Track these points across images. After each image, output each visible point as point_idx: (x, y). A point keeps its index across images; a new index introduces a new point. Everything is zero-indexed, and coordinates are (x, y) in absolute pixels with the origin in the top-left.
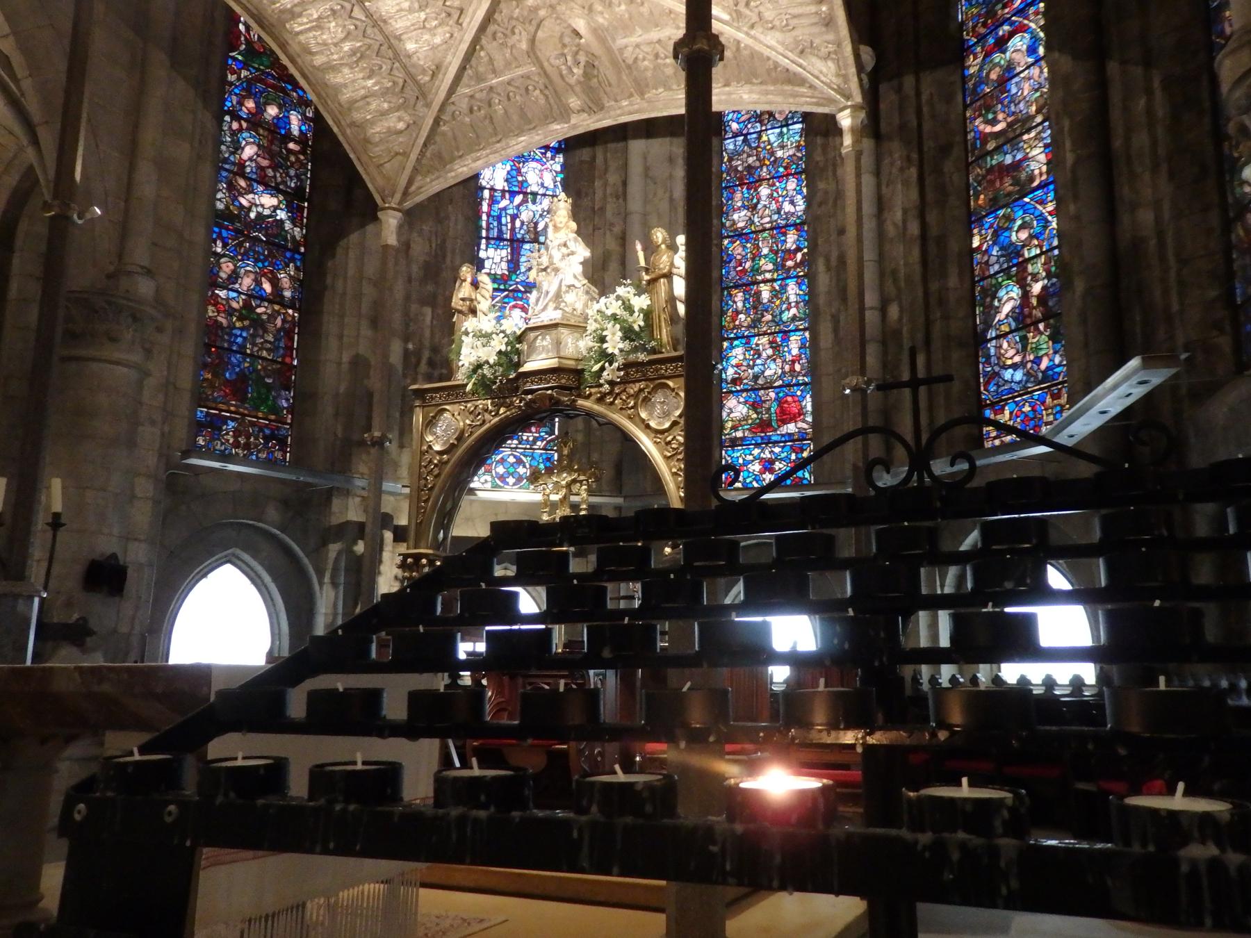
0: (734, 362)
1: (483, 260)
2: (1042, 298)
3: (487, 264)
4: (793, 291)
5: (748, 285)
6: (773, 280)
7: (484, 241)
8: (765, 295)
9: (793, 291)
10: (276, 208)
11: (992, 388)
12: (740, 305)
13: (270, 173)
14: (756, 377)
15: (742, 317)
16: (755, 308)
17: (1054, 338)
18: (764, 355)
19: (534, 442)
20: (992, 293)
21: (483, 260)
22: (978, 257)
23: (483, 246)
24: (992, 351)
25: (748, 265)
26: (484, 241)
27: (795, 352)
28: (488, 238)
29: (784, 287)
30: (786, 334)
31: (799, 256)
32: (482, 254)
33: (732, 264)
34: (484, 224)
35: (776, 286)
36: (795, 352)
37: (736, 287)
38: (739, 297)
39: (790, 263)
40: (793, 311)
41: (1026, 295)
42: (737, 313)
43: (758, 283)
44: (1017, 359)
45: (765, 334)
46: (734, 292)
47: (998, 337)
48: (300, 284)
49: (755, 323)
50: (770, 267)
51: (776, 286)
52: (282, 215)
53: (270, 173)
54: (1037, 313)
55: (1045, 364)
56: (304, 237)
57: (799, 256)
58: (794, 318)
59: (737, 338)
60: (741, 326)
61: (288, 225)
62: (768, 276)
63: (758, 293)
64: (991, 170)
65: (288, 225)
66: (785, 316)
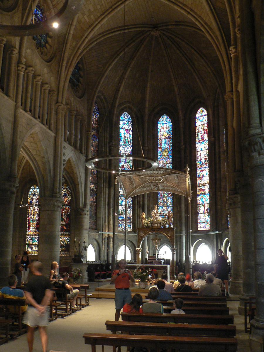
0: (160, 210)
1: (120, 192)
2: (207, 210)
3: (120, 192)
4: (170, 200)
5: (162, 198)
6: (167, 198)
7: (120, 188)
8: (165, 200)
9: (170, 200)
10: (93, 187)
11: (199, 220)
12: (161, 201)
13: (93, 181)
14: (164, 214)
15: (161, 203)
16: (164, 202)
17: (208, 216)
18: (165, 210)
19: (128, 223)
20: (200, 207)
21: (120, 192)
22: (198, 201)
23: (120, 189)
24: (200, 215)
25: (162, 195)
26: (120, 188)
27: (170, 210)
28: (121, 188)
29: (168, 199)
30: (169, 207)
31: (171, 195)
32: (120, 191)
33: (160, 194)
34: (120, 185)
35: (167, 199)
36: (170, 210)
37: (160, 198)
38: (161, 200)
39: (169, 195)
40: (170, 203)
41: (205, 209)
42: (161, 202)
43: (164, 198)
44: (203, 217)
45: (165, 207)
46: (160, 199)
47: (201, 213)
48: (96, 199)
49: (163, 205)
50: (166, 196)
51: (167, 199)
52: (94, 188)
53: (93, 181)
54: (206, 212)
55: (207, 219)
56: (97, 190)
57: (171, 195)
58: (170, 205)
59: (161, 207)
60: (161, 205)
61: (95, 189)
62: (166, 197)
63: (164, 200)
64: (200, 189)
65: (95, 189)
66: (169, 204)
